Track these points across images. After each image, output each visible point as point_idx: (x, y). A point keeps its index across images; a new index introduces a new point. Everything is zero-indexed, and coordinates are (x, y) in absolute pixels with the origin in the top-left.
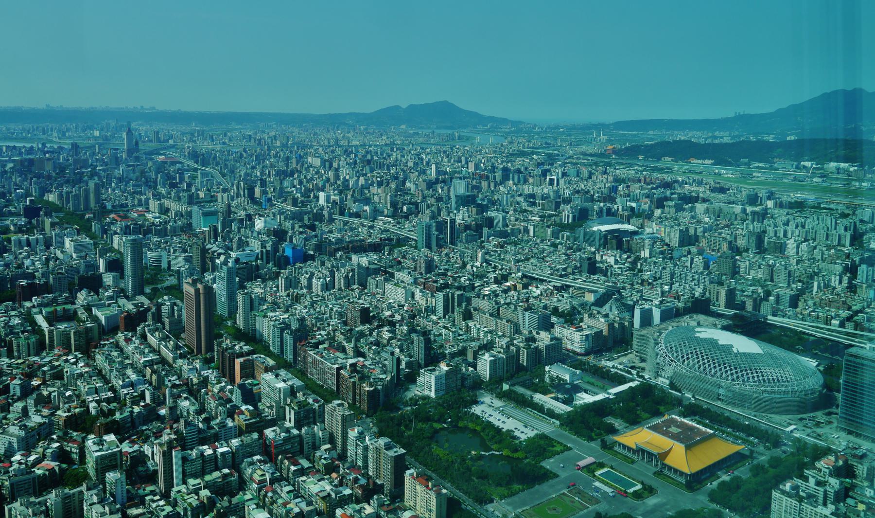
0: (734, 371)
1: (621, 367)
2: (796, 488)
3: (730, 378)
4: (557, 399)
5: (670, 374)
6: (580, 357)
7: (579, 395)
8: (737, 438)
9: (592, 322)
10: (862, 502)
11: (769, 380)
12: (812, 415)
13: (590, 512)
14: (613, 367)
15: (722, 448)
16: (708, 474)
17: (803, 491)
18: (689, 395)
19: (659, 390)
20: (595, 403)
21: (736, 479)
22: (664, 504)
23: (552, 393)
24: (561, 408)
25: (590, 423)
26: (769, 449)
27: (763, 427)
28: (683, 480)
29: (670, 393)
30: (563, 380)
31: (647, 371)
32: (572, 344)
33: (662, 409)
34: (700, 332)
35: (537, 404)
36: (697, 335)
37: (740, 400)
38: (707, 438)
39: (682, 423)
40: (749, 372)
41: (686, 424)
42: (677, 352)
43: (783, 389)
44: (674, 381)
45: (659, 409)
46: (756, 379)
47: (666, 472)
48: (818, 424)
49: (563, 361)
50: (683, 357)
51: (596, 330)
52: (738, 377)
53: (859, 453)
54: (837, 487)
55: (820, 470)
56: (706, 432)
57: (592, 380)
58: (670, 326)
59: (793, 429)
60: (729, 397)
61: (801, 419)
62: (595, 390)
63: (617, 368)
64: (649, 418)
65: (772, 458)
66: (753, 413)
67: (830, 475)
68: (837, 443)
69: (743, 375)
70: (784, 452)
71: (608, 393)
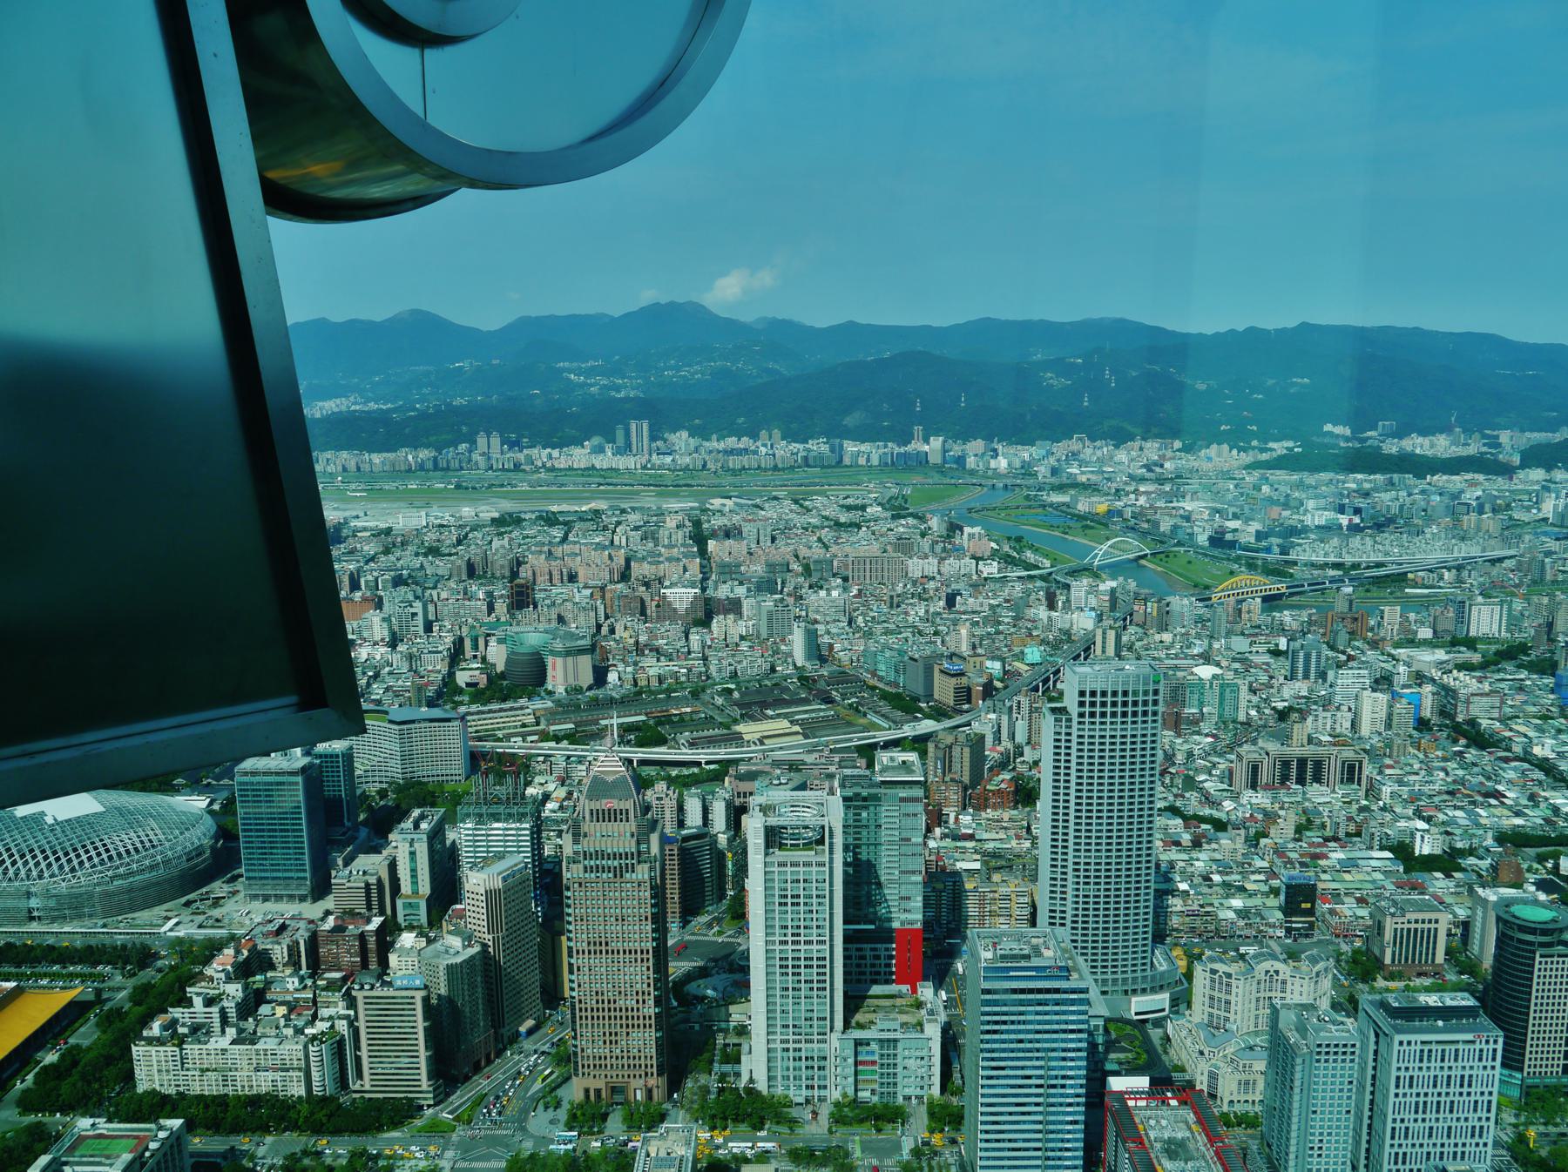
8: (72, 976)
11: (119, 855)
12: (204, 890)
17: (184, 1025)
26: (135, 974)
37: (73, 906)
40: (81, 851)
43: (147, 862)
46: (96, 860)
48: (217, 902)
54: (240, 994)
55: (212, 979)
59: (173, 925)
61: (188, 904)
67: (229, 979)
70: (160, 970)
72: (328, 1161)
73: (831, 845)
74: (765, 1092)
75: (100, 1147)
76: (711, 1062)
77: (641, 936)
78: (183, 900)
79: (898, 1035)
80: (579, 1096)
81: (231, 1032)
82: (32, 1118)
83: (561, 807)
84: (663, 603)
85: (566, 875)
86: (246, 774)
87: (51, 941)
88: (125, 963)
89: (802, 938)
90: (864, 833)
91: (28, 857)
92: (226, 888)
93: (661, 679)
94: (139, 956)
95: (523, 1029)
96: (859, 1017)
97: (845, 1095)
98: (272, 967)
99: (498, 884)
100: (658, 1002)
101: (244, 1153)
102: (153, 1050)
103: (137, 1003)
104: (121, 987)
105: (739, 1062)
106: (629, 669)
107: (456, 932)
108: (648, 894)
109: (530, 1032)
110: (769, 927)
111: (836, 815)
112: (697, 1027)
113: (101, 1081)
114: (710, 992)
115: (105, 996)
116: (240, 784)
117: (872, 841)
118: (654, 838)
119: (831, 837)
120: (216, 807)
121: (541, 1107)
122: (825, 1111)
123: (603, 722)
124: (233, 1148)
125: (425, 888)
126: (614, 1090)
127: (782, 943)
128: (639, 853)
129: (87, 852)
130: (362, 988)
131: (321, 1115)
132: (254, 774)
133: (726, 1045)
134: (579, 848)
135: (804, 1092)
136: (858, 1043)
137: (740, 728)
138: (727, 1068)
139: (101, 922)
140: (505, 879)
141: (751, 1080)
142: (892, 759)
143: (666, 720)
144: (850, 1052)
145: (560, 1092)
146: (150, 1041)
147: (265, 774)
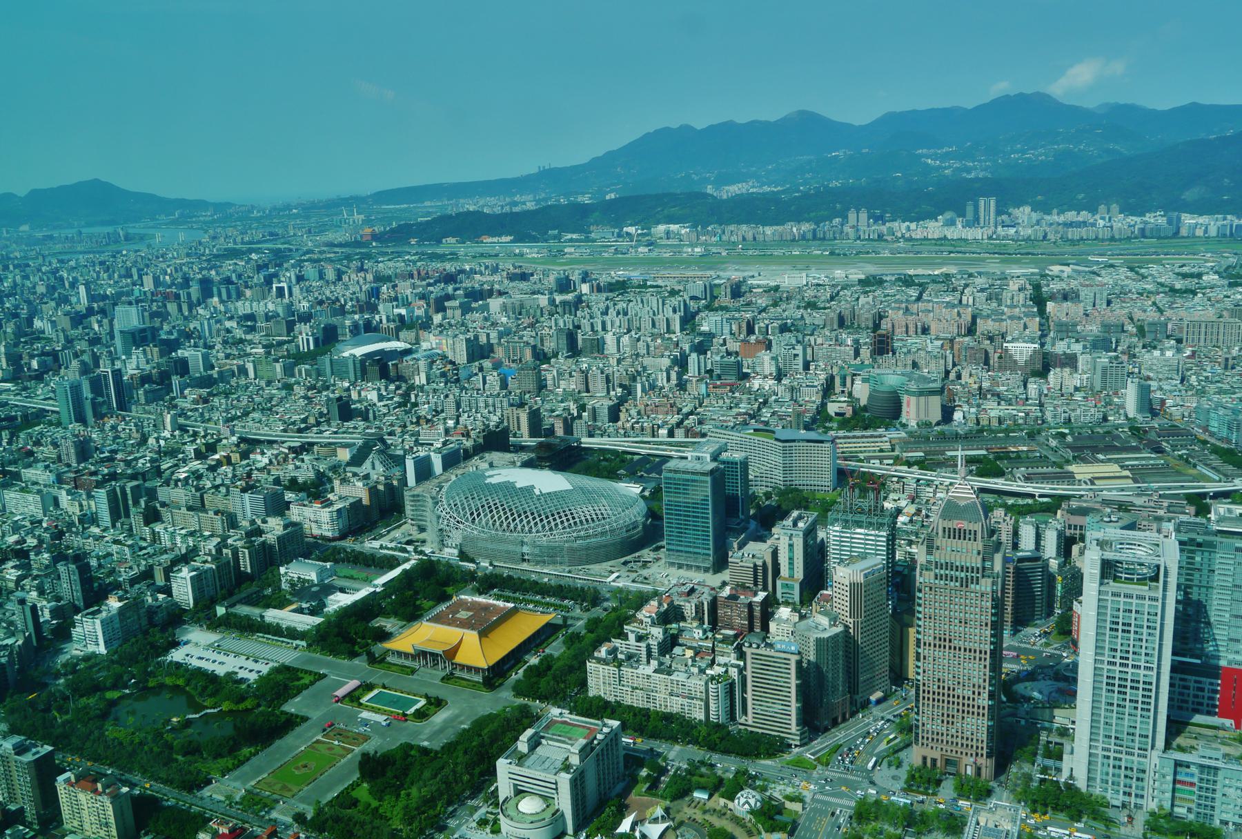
1: (393, 545)
2: (614, 651)
4: (300, 611)
5: (459, 541)
7: (332, 597)
8: (548, 605)
10: (690, 648)
11: (581, 522)
13: (356, 756)
14: (382, 547)
18: (485, 564)
20: (355, 604)
22: (457, 716)
23: (291, 603)
24: (306, 622)
25: (351, 634)
27: (579, 584)
28: (478, 678)
29: (459, 567)
32: (320, 527)
33: (449, 590)
35: (270, 625)
36: (488, 481)
37: (550, 555)
38: (507, 615)
39: (473, 603)
41: (479, 604)
42: (464, 509)
44: (464, 549)
47: (458, 673)
48: (645, 565)
50: (472, 514)
51: (351, 500)
54: (661, 637)
56: (504, 608)
57: (354, 572)
59: (615, 577)
61: (625, 563)
62: (355, 585)
63: (387, 548)
67: (653, 624)
69: (549, 522)
70: (605, 610)
72: (720, 773)
73: (1165, 583)
74: (1084, 790)
75: (564, 732)
76: (1035, 754)
77: (982, 638)
78: (623, 560)
79: (1219, 764)
80: (918, 762)
81: (654, 663)
82: (521, 701)
83: (911, 521)
84: (1005, 357)
85: (919, 579)
86: (670, 471)
89: (1130, 662)
90: (1197, 575)
92: (653, 555)
93: (1000, 421)
94: (590, 597)
95: (873, 698)
96: (1180, 740)
97: (1161, 807)
98: (684, 619)
99: (860, 579)
100: (991, 696)
101: (659, 755)
102: (601, 667)
103: (590, 631)
104: (580, 619)
105: (1060, 758)
106: (973, 410)
107: (825, 614)
108: (989, 604)
109: (879, 702)
110: (1099, 649)
111: (1171, 557)
112: (1023, 722)
113: (563, 682)
114: (1036, 694)
116: (666, 478)
117: (1204, 583)
118: (998, 558)
119: (1166, 575)
120: (647, 493)
121: (885, 763)
122: (1141, 818)
123: (949, 453)
124: (652, 749)
125: (799, 574)
126: (948, 762)
127: (1110, 663)
128: (984, 568)
130: (750, 646)
131: (715, 737)
132: (676, 472)
133: (1049, 742)
134: (931, 558)
135: (1121, 797)
136: (1178, 764)
137: (1072, 468)
138: (1049, 762)
140: (866, 576)
141: (1071, 777)
142: (1230, 511)
143: (1006, 456)
144: (1169, 770)
145: (902, 755)
146: (599, 660)
147: (684, 472)
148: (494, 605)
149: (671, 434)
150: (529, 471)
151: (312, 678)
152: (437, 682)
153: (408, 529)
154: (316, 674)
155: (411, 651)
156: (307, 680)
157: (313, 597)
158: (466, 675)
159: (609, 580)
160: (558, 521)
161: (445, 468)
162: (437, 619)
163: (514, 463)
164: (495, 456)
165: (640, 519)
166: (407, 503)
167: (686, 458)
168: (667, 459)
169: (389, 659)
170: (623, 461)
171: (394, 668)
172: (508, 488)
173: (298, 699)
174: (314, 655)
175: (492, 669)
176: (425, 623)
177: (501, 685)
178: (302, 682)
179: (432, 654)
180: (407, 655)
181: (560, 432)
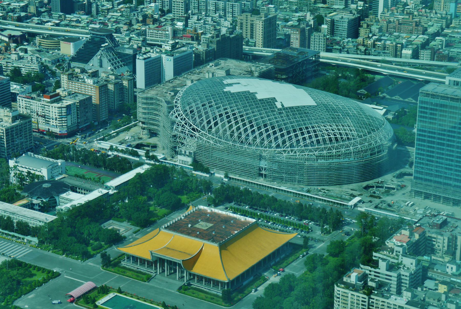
0: (278, 134)
1: (123, 147)
2: (364, 278)
3: (274, 145)
4: (31, 206)
5: (193, 149)
6: (60, 141)
7: (64, 195)
8: (286, 224)
9: (75, 86)
11: (324, 140)
12: (380, 179)
14: (111, 149)
15: (270, 240)
16: (252, 278)
17: (372, 280)
18: (220, 175)
19: (179, 173)
20: (88, 204)
21: (288, 279)
23: (24, 198)
26: (329, 232)
27: (319, 204)
29: (192, 175)
30: (38, 177)
31: (159, 149)
32: (47, 123)
33: (184, 198)
34: (231, 85)
36: (227, 89)
37: (288, 172)
38: (248, 229)
39: (213, 215)
40: (298, 132)
42: (200, 116)
43: (343, 150)
44: (198, 158)
45: (180, 200)
49: (36, 150)
50: (209, 122)
51: (81, 97)
52: (284, 142)
53: (438, 220)
54: (413, 268)
55: (392, 250)
56: (245, 223)
57: (82, 172)
58: (189, 81)
60: (274, 171)
62: (87, 185)
63: (117, 150)
64: (167, 214)
65: (332, 243)
66: (306, 188)
67: (405, 254)
68: (412, 212)
69: (290, 138)
70: (347, 234)
71: (107, 188)
78: (365, 184)
86: (428, 95)
87: (272, 194)
88: (325, 222)
91: (263, 130)
92: (396, 181)
98: (432, 251)
102: (350, 293)
104: (322, 242)
115: (310, 243)
116: (422, 102)
120: (390, 117)
129: (302, 134)
132: (433, 96)
139: (306, 188)
146: (348, 286)
147: (443, 97)
148: (235, 219)
149: (416, 55)
150: (268, 83)
151: (45, 275)
152: (174, 291)
153: (135, 133)
154: (49, 272)
155: (149, 257)
156: (39, 277)
157: (46, 193)
158: (203, 287)
159: (352, 203)
160: (300, 137)
161: (178, 72)
162: (176, 228)
163: (250, 74)
164: (232, 64)
165: (387, 143)
166: (139, 104)
167: (444, 83)
168: (427, 82)
169: (123, 264)
170: (363, 80)
171: (129, 273)
172: (248, 98)
173: (31, 296)
174: (46, 252)
175: (232, 283)
176: (163, 231)
177: (240, 300)
178: (35, 278)
179: (171, 263)
180: (143, 261)
181: (295, 43)
